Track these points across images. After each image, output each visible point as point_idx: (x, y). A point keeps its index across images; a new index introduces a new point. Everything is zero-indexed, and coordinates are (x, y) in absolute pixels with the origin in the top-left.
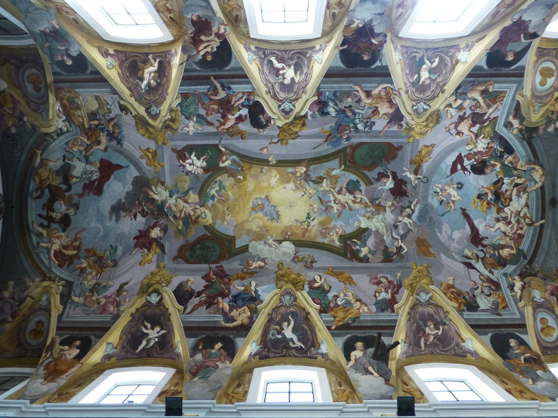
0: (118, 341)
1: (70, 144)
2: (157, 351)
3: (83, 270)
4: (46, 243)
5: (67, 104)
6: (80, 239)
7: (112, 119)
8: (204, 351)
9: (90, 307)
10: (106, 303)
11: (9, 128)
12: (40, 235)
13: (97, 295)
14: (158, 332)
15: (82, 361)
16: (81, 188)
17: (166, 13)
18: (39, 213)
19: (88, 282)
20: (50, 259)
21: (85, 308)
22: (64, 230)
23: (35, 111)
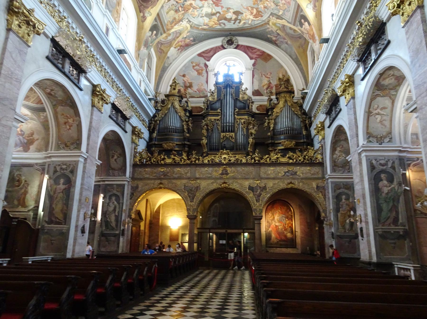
3: (265, 7)
4: (249, 21)
5: (174, 24)
6: (247, 7)
7: (177, 2)
9: (286, 9)
12: (245, 23)
16: (218, 8)
17: (118, 11)
20: (258, 20)
22: (242, 14)
23: (180, 34)
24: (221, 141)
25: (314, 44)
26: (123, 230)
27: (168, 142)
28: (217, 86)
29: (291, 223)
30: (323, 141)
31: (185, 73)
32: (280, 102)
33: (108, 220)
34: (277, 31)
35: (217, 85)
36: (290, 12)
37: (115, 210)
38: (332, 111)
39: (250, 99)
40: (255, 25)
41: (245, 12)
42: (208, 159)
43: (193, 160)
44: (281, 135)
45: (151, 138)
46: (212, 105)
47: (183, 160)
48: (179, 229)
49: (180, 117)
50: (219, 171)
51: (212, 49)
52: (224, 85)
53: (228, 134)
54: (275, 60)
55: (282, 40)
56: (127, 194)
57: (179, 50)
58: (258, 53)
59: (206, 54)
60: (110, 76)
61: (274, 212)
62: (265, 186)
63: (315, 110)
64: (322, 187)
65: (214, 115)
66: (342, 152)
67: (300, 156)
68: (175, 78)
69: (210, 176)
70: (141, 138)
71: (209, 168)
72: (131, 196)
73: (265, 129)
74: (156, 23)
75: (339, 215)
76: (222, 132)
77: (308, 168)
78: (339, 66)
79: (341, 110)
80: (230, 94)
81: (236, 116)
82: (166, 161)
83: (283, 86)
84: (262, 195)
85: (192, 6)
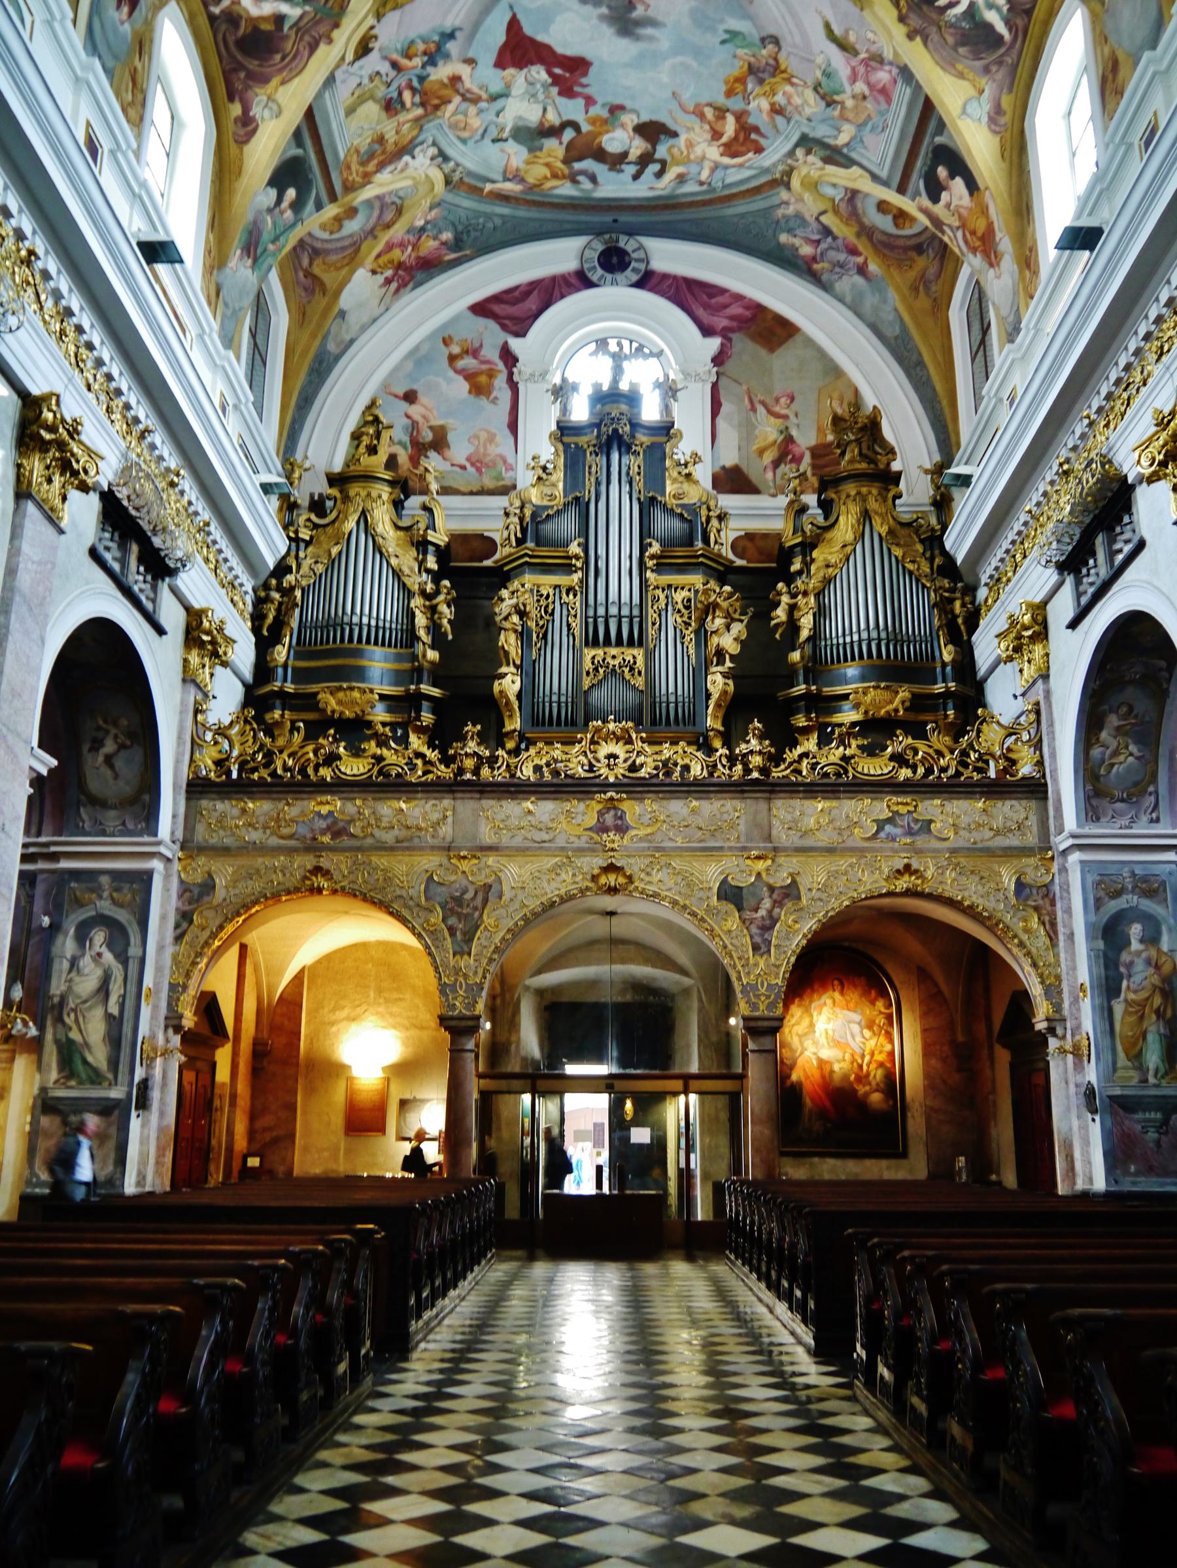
0: (965, 83)
1: (465, 134)
3: (777, 110)
5: (375, 162)
6: (697, 105)
7: (395, 65)
9: (869, 117)
10: (868, 84)
11: (444, 244)
12: (681, 179)
15: (981, 186)
17: (139, 80)
18: (630, 179)
19: (808, 105)
20: (741, 166)
23: (399, 212)
24: (587, 682)
26: (145, 1085)
27: (345, 685)
28: (563, 444)
29: (888, 1047)
30: (1040, 682)
31: (415, 387)
32: (841, 518)
33: (74, 1035)
34: (823, 219)
35: (562, 435)
37: (104, 989)
38: (1093, 554)
39: (712, 504)
40: (725, 187)
41: (689, 129)
42: (537, 761)
43: (469, 763)
44: (846, 660)
45: (263, 669)
46: (541, 527)
47: (419, 762)
48: (388, 1080)
49: (397, 574)
50: (584, 814)
51: (533, 286)
52: (598, 436)
53: (613, 651)
54: (810, 343)
55: (842, 257)
56: (163, 917)
57: (388, 281)
58: (736, 310)
59: (503, 306)
60: (99, 363)
61: (811, 1002)
62: (794, 882)
63: (1000, 554)
64: (1039, 887)
65: (547, 569)
66: (1126, 734)
67: (946, 752)
68: (373, 404)
69: (546, 837)
70: (225, 664)
72: (177, 926)
73: (777, 636)
74: (300, 152)
75: (1118, 1008)
76: (587, 644)
77: (980, 804)
78: (1138, 352)
79: (1141, 545)
80: (624, 478)
81: (649, 574)
82: (343, 769)
83: (852, 453)
84: (778, 925)
85: (459, 86)
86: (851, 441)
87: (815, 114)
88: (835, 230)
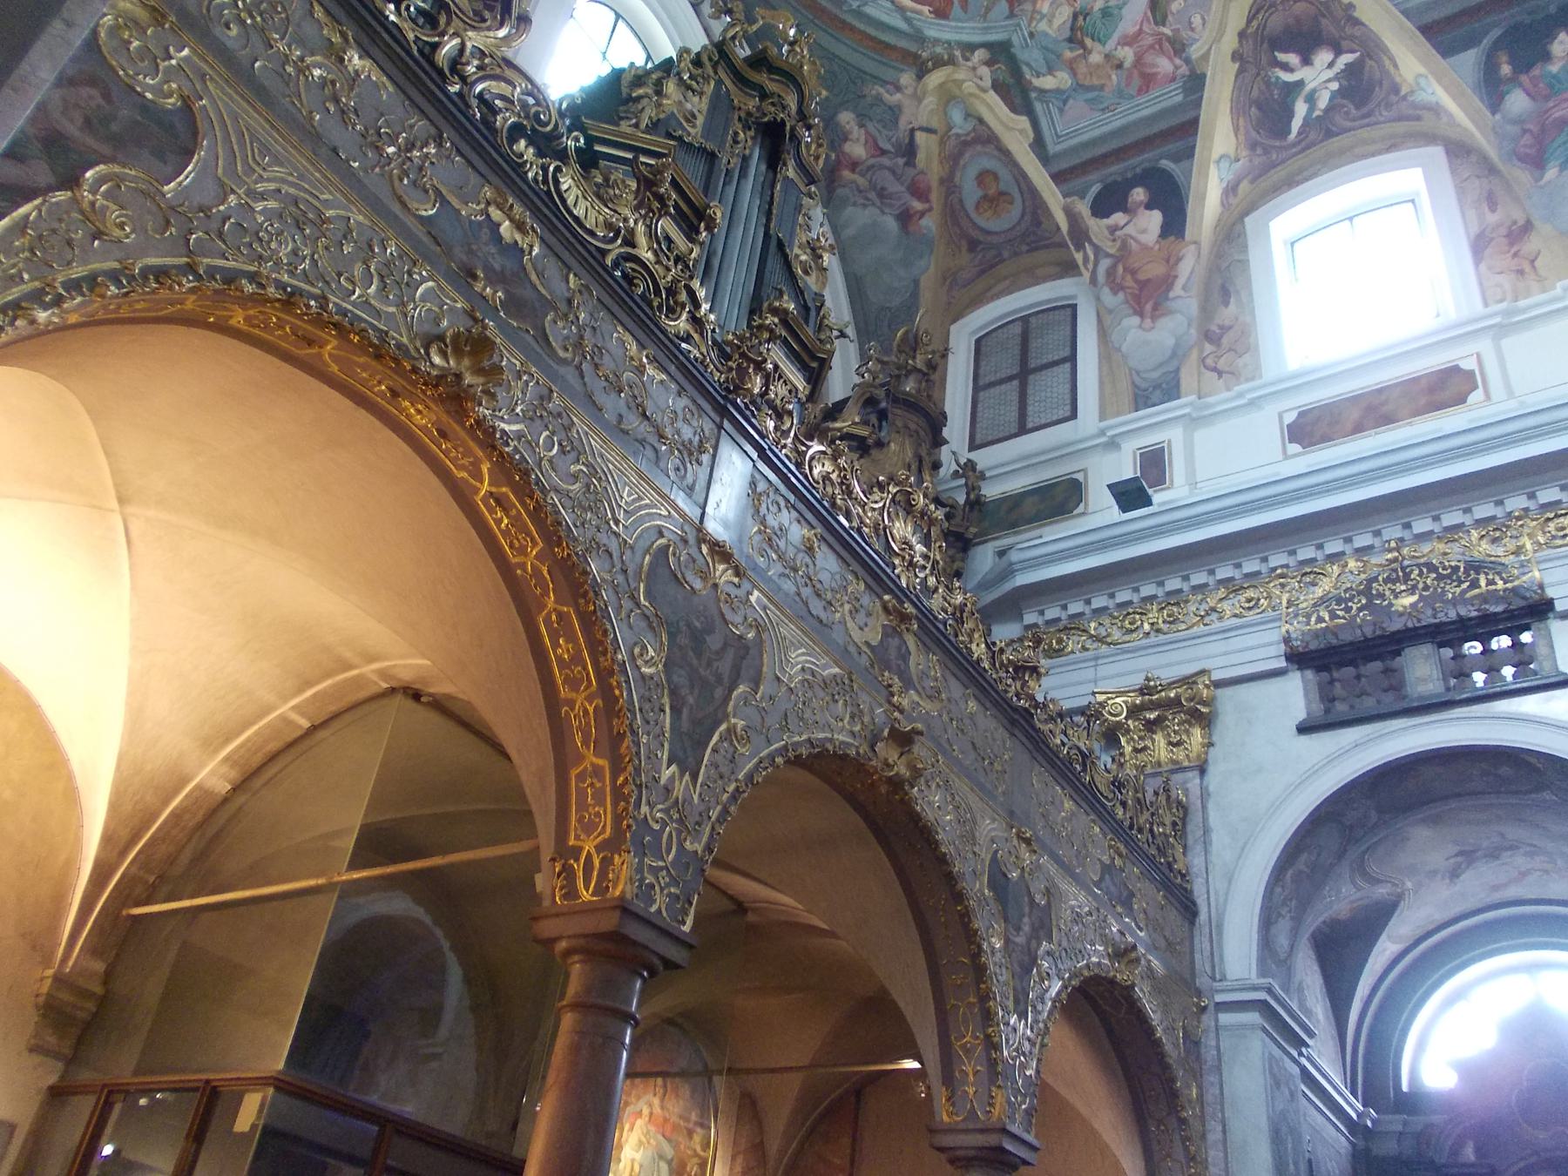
2: (1347, 113)
8: (1524, 78)
9: (1102, 88)
10: (1139, 60)
13: (1098, 47)
14: (1331, 65)
19: (1050, 21)
21: (1090, 95)
25: (1136, 320)
34: (920, 137)
36: (1097, 116)
40: (859, 14)
55: (894, 187)
71: (824, 548)
86: (919, 371)
87: (1046, 34)
88: (921, 157)
